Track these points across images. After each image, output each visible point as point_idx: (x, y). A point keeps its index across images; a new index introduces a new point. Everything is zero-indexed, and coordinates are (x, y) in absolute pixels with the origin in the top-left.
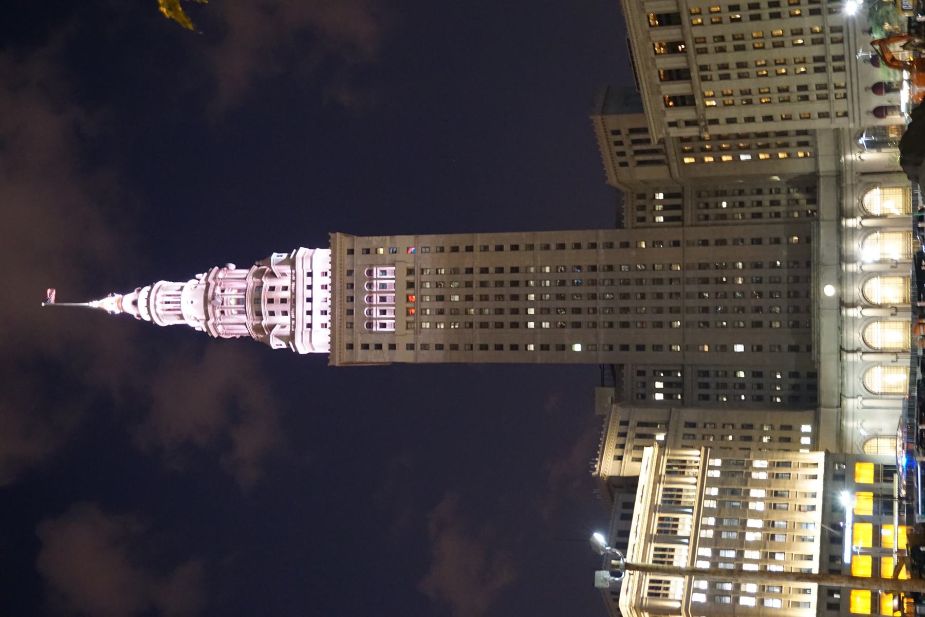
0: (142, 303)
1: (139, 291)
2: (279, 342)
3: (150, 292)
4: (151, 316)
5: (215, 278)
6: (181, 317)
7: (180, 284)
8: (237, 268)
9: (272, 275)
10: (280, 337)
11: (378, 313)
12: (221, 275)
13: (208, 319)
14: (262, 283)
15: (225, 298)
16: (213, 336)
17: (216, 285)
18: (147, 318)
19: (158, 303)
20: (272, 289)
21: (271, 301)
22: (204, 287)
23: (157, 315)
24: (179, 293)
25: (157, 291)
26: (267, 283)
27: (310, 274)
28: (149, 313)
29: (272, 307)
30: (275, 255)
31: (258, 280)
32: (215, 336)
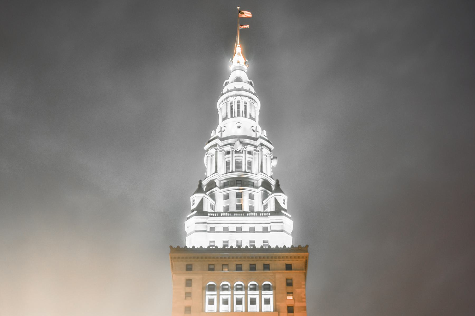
0: (239, 85)
1: (251, 84)
2: (197, 202)
3: (249, 91)
5: (262, 145)
7: (257, 119)
8: (273, 168)
9: (265, 196)
10: (201, 203)
11: (225, 297)
12: (265, 151)
13: (222, 139)
14: (257, 188)
15: (243, 155)
17: (256, 147)
18: (225, 90)
19: (238, 98)
20: (251, 197)
21: (239, 195)
22: (254, 136)
24: (248, 116)
25: (250, 98)
27: (265, 230)
28: (228, 91)
31: (260, 184)
32: (206, 148)
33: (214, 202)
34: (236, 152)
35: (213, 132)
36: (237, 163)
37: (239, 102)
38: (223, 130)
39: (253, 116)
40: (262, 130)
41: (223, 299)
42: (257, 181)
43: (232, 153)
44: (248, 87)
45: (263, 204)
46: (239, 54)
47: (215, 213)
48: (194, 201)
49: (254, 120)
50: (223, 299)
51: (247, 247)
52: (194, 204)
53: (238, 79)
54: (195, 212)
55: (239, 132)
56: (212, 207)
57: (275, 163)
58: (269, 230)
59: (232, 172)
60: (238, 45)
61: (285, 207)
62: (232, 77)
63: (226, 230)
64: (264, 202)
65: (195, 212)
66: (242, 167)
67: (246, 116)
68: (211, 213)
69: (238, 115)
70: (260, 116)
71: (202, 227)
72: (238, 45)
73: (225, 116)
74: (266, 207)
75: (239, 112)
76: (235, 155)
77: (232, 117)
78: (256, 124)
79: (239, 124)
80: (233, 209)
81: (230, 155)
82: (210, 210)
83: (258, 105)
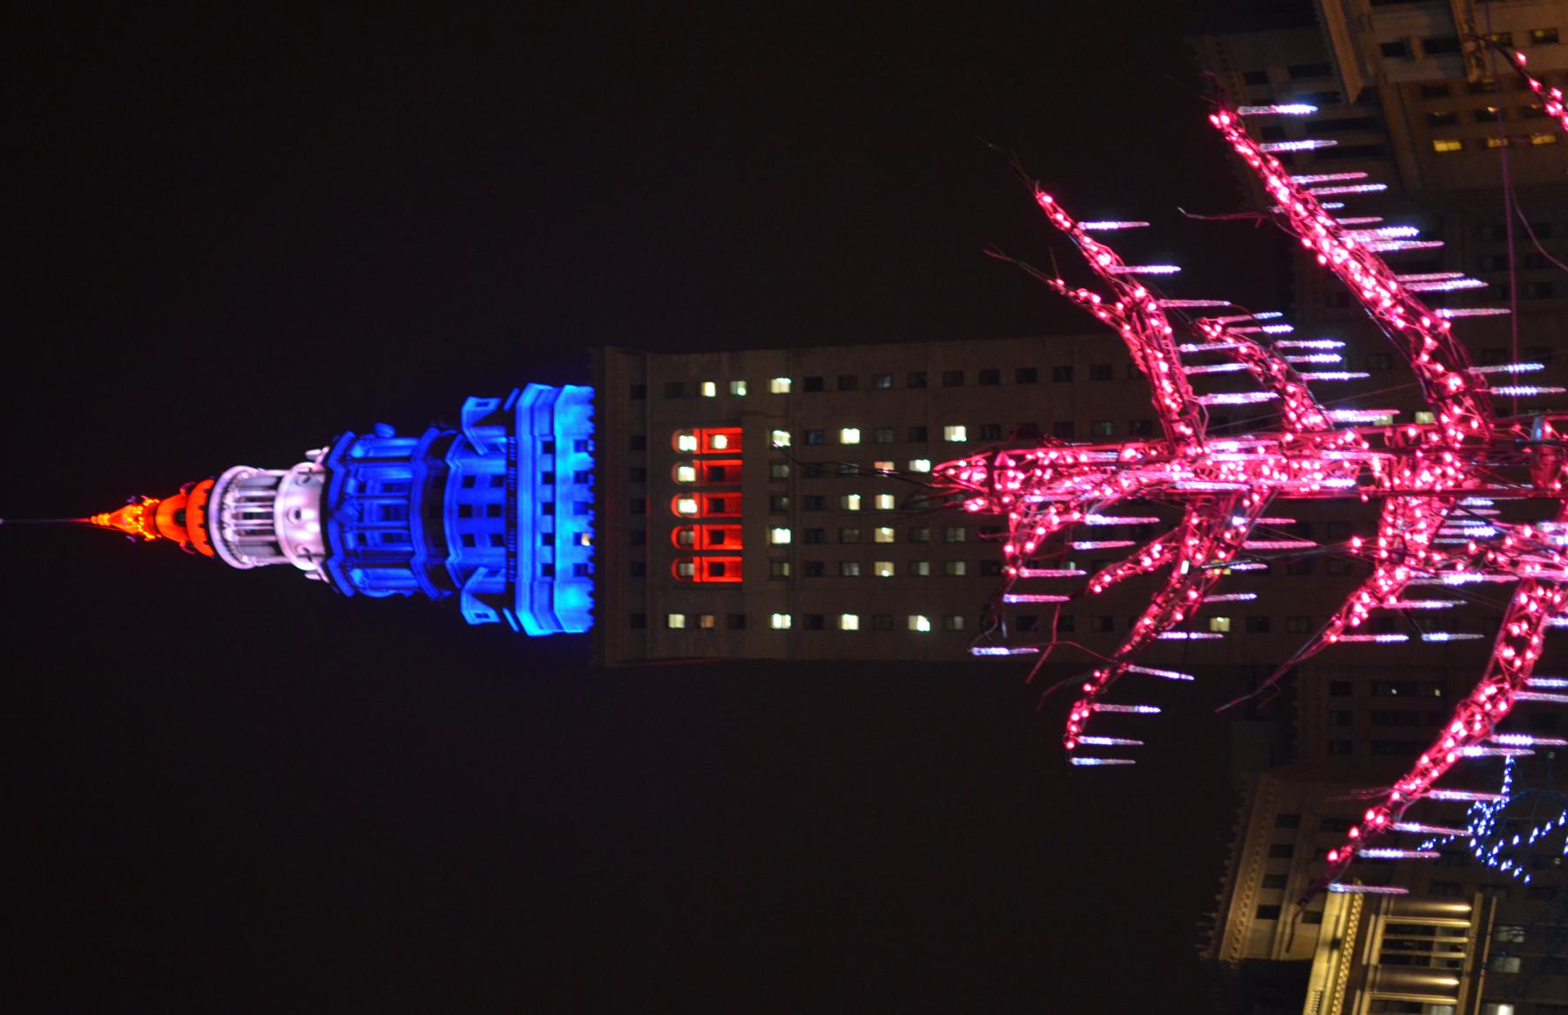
0: (194, 516)
1: (190, 490)
2: (481, 608)
3: (209, 492)
4: (213, 548)
6: (276, 548)
7: (278, 473)
8: (397, 436)
9: (468, 449)
10: (481, 596)
11: (706, 541)
12: (358, 452)
14: (448, 468)
15: (367, 504)
16: (342, 594)
18: (206, 550)
19: (227, 517)
20: (469, 481)
21: (466, 511)
22: (321, 479)
23: (225, 542)
24: (272, 493)
25: (225, 491)
26: (456, 464)
27: (550, 448)
28: (209, 541)
29: (471, 526)
30: (470, 405)
33: (482, 570)
34: (360, 519)
35: (309, 576)
36: (386, 517)
37: (235, 516)
38: (302, 552)
39: (271, 482)
40: (306, 460)
41: (712, 543)
42: (430, 468)
43: (365, 528)
44: (198, 496)
45: (486, 456)
46: (119, 519)
47: (508, 568)
48: (478, 616)
49: (280, 479)
50: (712, 543)
51: (591, 489)
52: (486, 616)
53: (179, 518)
54: (507, 614)
55: (311, 515)
56: (493, 572)
57: (388, 431)
58: (549, 439)
59: (408, 528)
60: (93, 520)
61: (493, 403)
62: (172, 534)
63: (549, 509)
64: (481, 452)
65: (507, 614)
66: (396, 506)
67: (272, 499)
68: (507, 575)
69: (270, 516)
70: (267, 468)
71: (541, 597)
72: (93, 520)
73: (269, 550)
74: (494, 450)
75: (258, 516)
76: (367, 521)
77: (273, 532)
78: (289, 476)
79: (292, 518)
80: (499, 525)
81: (368, 534)
82: (500, 579)
83: (244, 472)
